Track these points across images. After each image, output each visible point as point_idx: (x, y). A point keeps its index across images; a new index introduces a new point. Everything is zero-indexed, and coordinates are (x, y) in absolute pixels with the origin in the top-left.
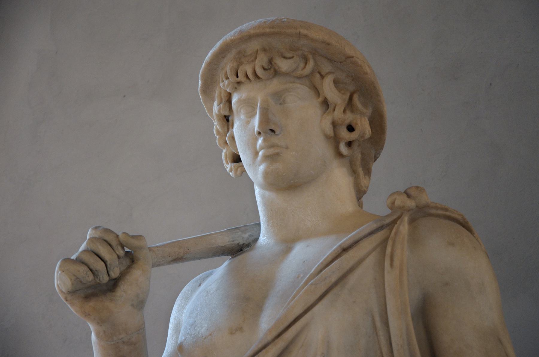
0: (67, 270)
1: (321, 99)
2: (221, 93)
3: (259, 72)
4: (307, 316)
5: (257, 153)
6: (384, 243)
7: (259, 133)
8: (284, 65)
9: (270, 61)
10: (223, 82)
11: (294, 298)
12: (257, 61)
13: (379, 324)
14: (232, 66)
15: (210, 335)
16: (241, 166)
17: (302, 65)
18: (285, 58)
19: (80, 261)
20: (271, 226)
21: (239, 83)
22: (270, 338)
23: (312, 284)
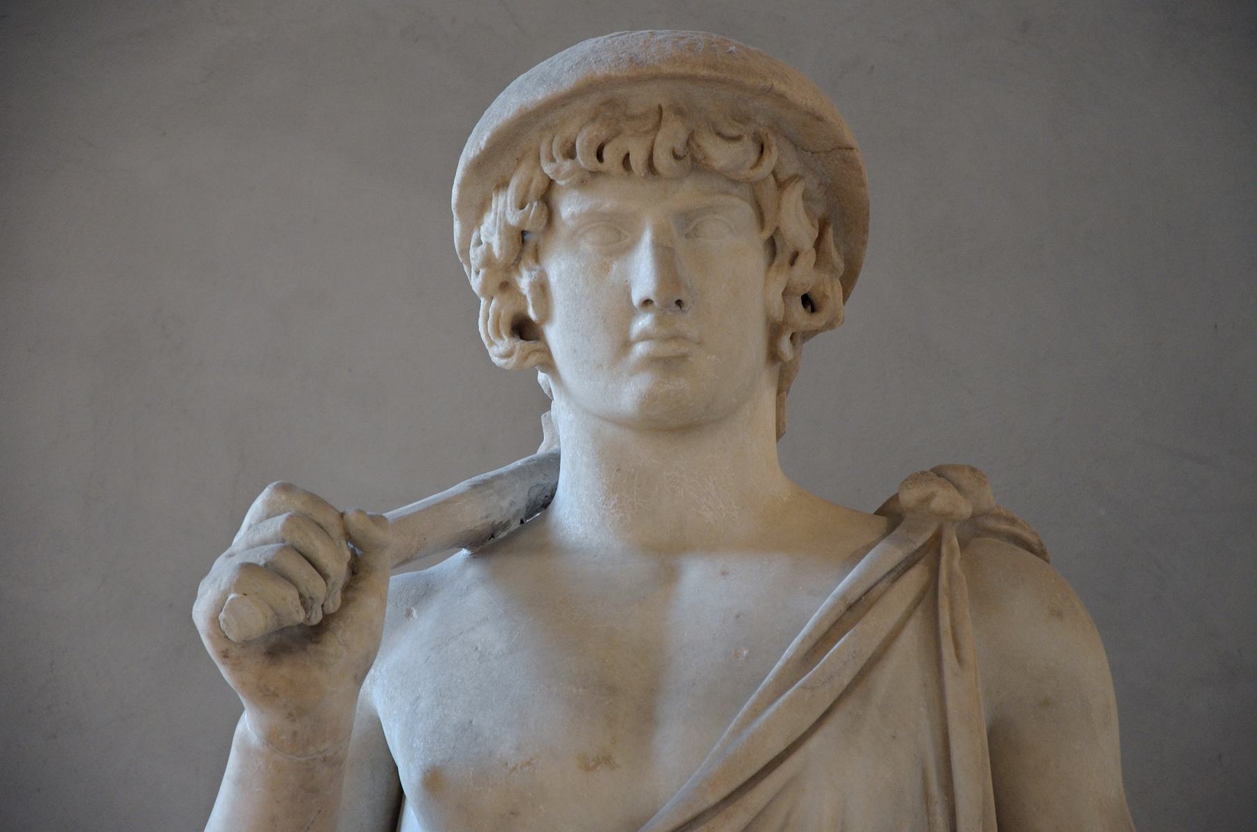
0: (257, 593)
2: (531, 181)
5: (626, 345)
7: (647, 302)
10: (553, 160)
12: (660, 137)
14: (596, 136)
15: (529, 763)
20: (615, 505)
22: (712, 799)
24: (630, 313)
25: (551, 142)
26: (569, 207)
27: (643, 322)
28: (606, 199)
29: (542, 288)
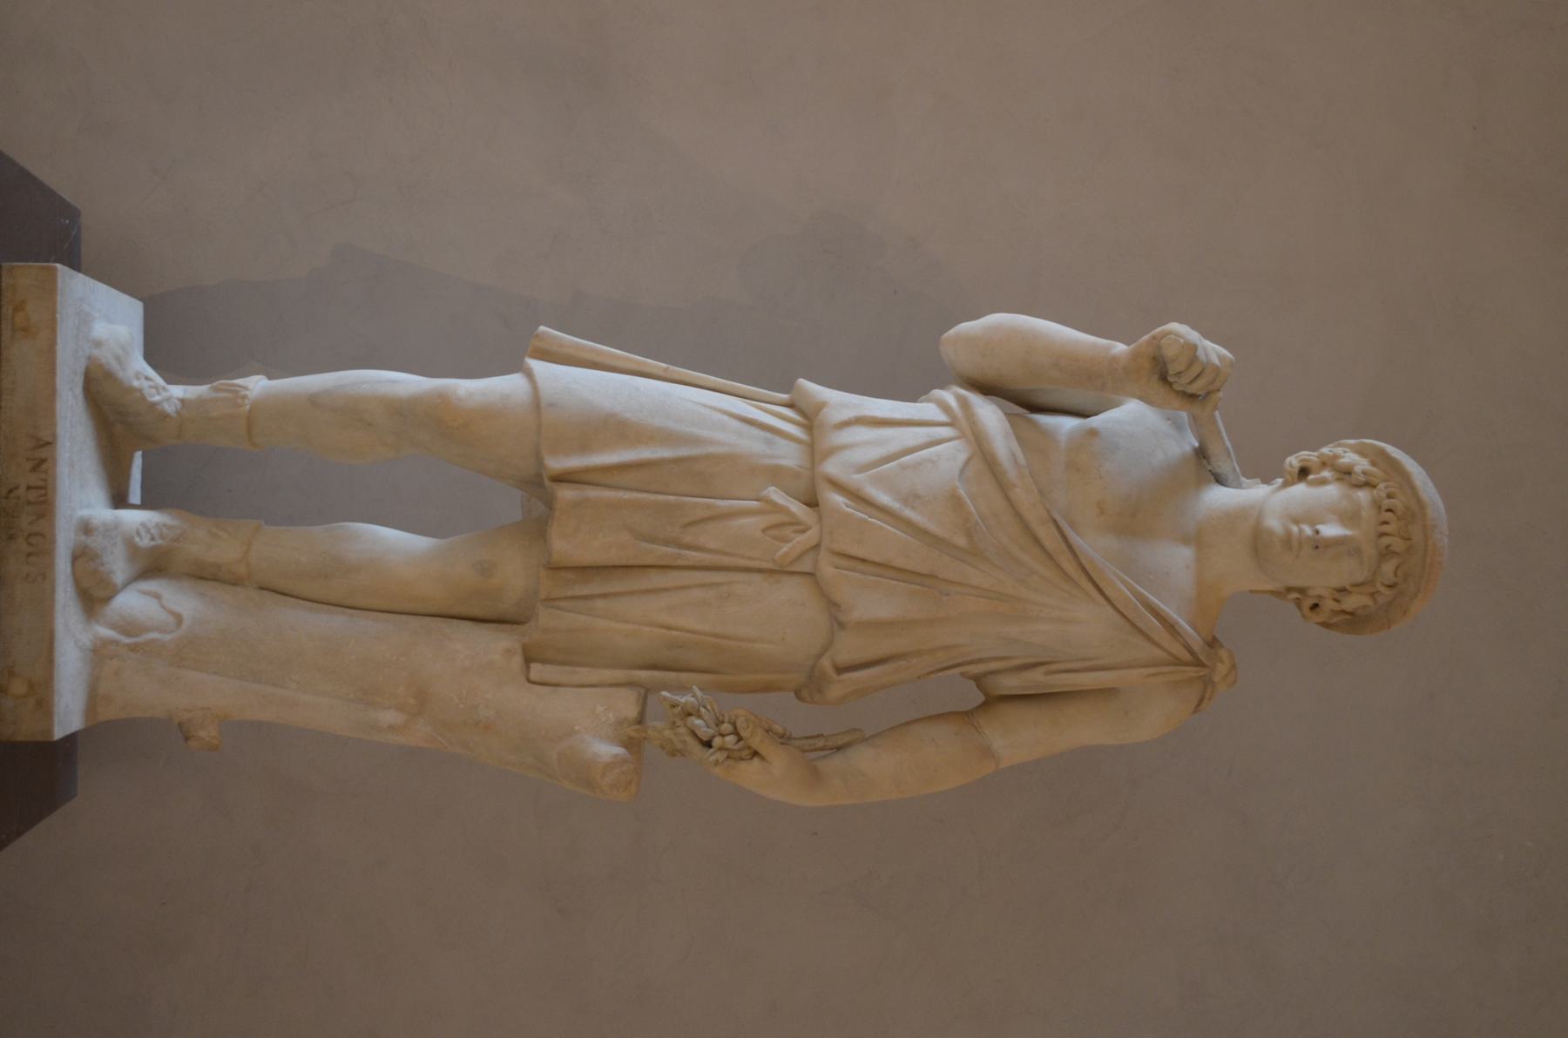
1: (1348, 588)
2: (1375, 477)
3: (1385, 541)
4: (1102, 601)
5: (1296, 522)
6: (1178, 662)
7: (1317, 532)
8: (1388, 567)
9: (1395, 553)
10: (1386, 488)
11: (1123, 582)
12: (1397, 539)
13: (1088, 664)
16: (1293, 480)
17: (1387, 583)
18: (1397, 567)
19: (1193, 359)
21: (1379, 508)
22: (1084, 561)
23: (1136, 605)
24: (1312, 524)
25: (1394, 487)
26: (1363, 496)
27: (1308, 531)
28: (1368, 513)
29: (1323, 482)
